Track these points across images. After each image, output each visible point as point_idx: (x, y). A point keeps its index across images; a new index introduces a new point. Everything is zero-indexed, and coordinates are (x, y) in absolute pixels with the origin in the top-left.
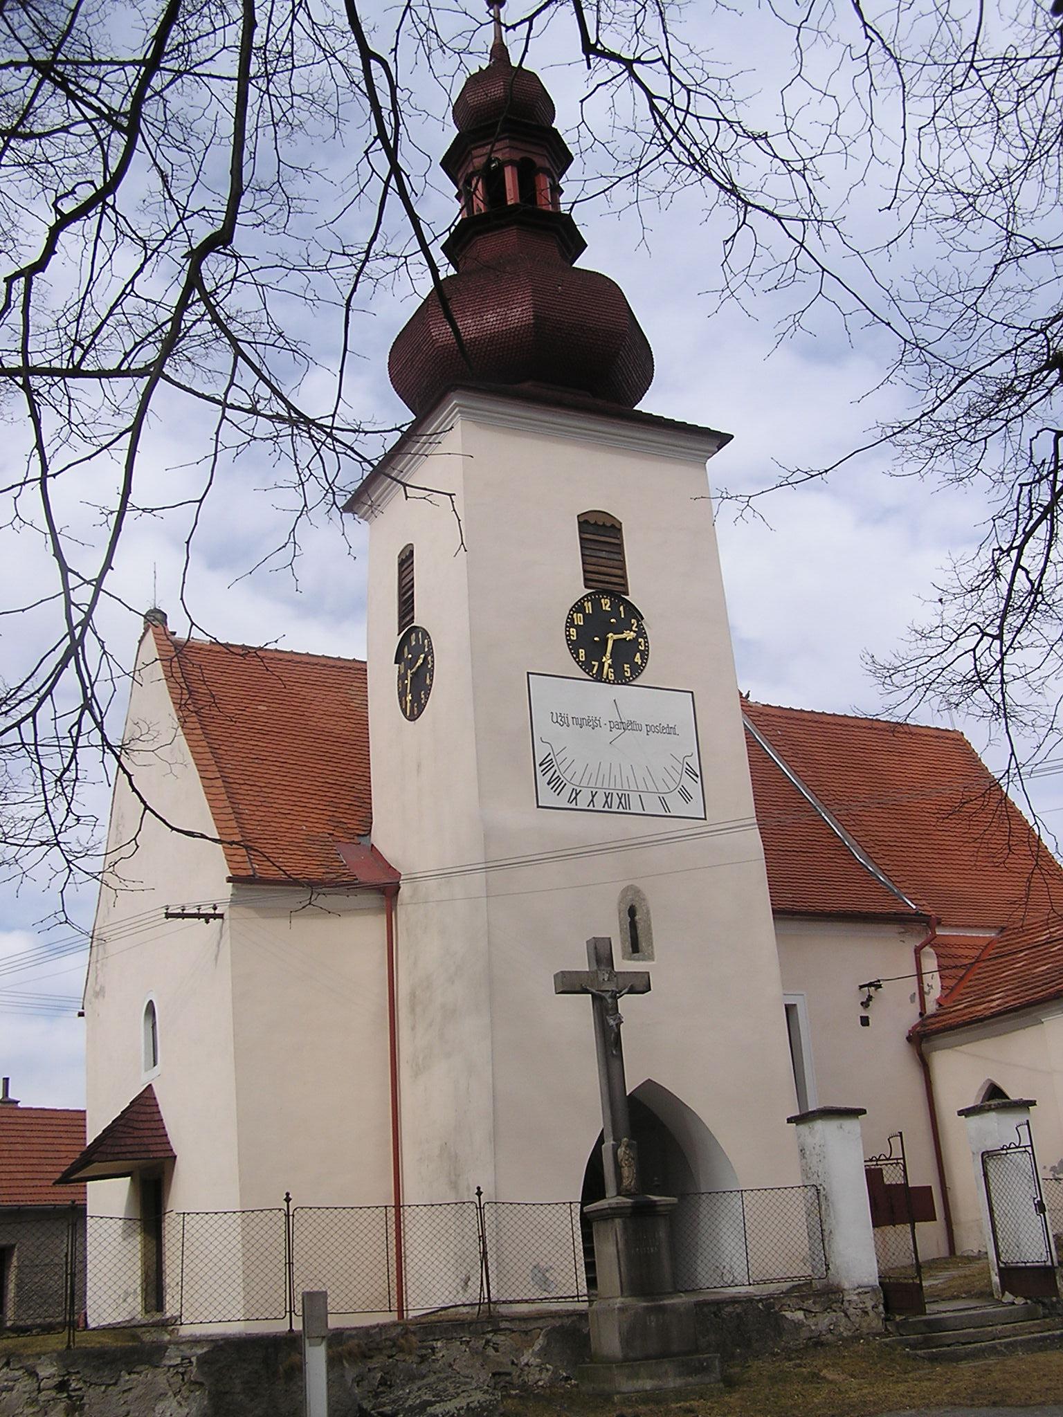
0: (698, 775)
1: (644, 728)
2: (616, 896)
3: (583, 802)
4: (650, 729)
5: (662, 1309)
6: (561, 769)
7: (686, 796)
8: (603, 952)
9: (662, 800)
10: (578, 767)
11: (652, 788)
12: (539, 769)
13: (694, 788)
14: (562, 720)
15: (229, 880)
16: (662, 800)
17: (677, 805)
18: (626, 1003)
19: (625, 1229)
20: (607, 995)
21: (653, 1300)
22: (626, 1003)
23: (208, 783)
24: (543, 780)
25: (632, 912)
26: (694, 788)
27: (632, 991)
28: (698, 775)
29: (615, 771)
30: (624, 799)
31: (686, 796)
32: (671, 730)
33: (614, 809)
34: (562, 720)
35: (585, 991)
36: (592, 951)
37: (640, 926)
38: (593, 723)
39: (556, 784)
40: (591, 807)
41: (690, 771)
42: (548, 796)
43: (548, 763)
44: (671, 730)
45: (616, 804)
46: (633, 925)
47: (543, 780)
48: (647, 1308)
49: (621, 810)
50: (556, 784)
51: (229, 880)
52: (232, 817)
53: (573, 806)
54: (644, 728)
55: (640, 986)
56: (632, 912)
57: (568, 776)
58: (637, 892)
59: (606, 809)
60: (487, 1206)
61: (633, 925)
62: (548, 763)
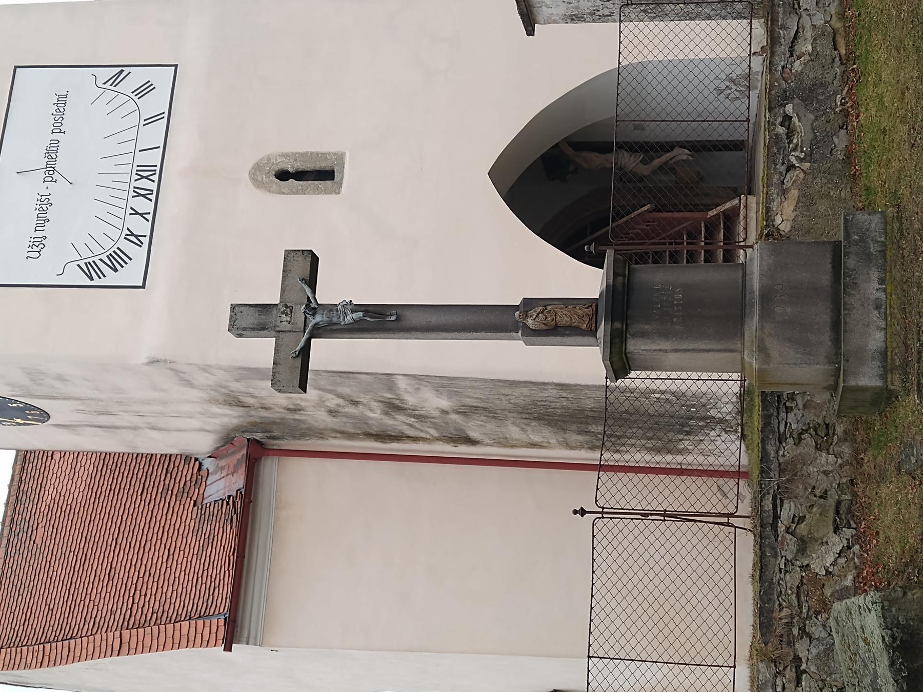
0: (121, 71)
1: (55, 136)
2: (262, 195)
3: (142, 227)
4: (58, 129)
5: (767, 296)
6: (99, 253)
7: (145, 89)
8: (250, 319)
9: (150, 121)
10: (99, 229)
11: (132, 134)
12: (97, 282)
13: (137, 77)
14: (38, 245)
15: (228, 648)
16: (150, 121)
17: (156, 103)
18: (325, 295)
19: (644, 335)
20: (312, 322)
21: (752, 305)
22: (325, 295)
23: (125, 648)
24: (112, 278)
25: (283, 175)
26: (137, 77)
27: (312, 282)
28: (121, 71)
29: (107, 180)
30: (143, 172)
31: (145, 89)
32: (61, 101)
33: (154, 186)
34: (38, 245)
35: (305, 353)
36: (255, 333)
37: (300, 166)
38: (44, 203)
39: (116, 260)
40: (150, 217)
41: (116, 80)
42: (131, 274)
43: (90, 269)
44: (61, 101)
45: (149, 180)
46: (300, 175)
47: (112, 278)
48: (762, 317)
49: (155, 178)
50: (116, 260)
51: (228, 648)
52: (162, 627)
53: (146, 241)
54: (55, 136)
55: (303, 267)
56: (283, 175)
57: (108, 244)
58: (257, 168)
59: (153, 197)
60: (601, 502)
61: (300, 175)
62: (90, 269)
